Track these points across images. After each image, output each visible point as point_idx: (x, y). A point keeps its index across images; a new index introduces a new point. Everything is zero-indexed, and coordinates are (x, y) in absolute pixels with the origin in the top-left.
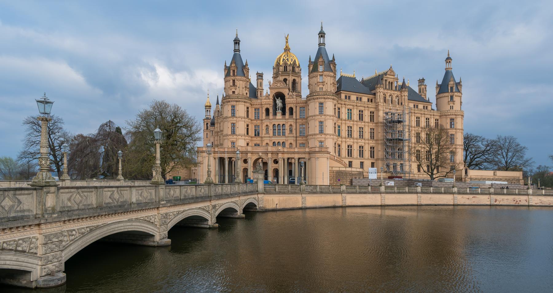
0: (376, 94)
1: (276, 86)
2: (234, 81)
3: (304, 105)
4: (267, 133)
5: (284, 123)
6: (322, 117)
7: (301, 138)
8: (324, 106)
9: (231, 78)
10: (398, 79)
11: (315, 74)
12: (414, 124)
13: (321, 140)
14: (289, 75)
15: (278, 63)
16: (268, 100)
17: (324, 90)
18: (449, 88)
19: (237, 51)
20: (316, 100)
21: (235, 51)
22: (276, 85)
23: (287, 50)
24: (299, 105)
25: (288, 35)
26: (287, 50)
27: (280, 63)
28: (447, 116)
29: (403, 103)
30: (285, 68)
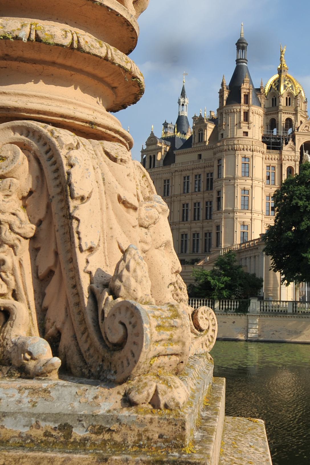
1: (307, 132)
2: (246, 114)
16: (293, 154)
19: (243, 62)
22: (307, 128)
26: (284, 71)
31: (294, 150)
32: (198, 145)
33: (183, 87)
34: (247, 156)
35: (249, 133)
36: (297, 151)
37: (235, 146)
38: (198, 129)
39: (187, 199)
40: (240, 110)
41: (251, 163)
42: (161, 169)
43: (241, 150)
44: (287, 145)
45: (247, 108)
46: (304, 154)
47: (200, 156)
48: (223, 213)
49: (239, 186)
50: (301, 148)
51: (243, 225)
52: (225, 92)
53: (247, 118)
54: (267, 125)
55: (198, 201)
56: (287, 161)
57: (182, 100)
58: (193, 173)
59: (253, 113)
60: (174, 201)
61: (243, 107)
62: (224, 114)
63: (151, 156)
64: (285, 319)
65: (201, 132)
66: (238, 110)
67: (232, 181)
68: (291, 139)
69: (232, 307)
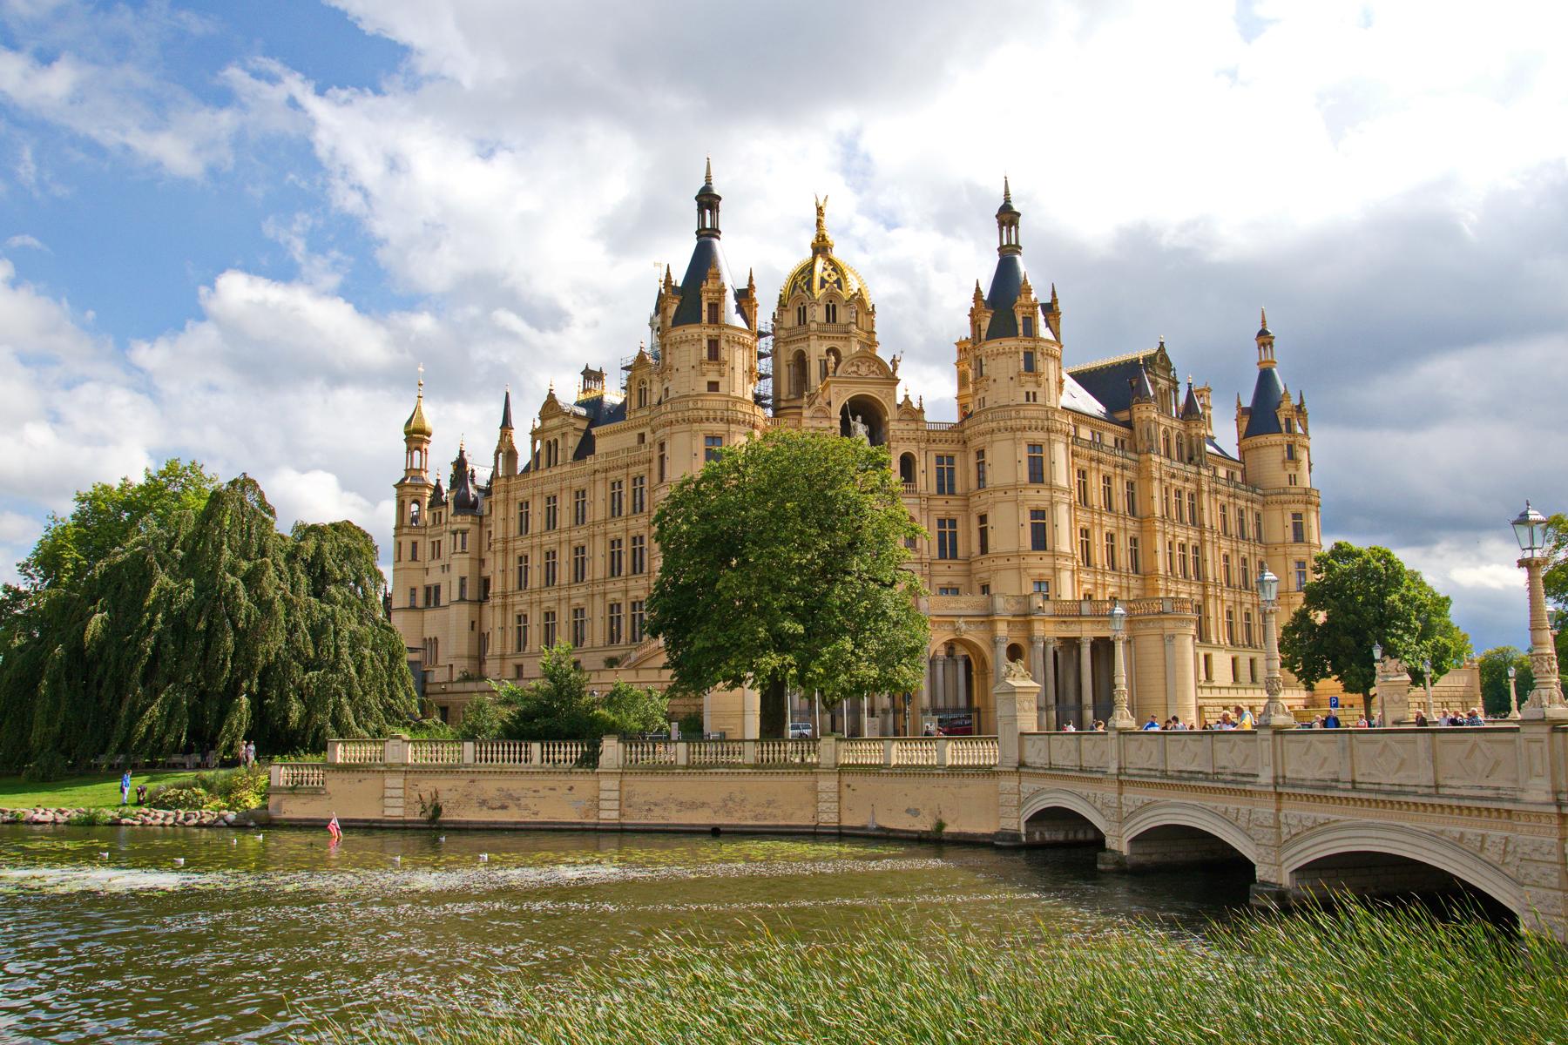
0: (1137, 429)
6: (1042, 493)
7: (945, 567)
8: (1045, 455)
9: (703, 331)
10: (1177, 383)
11: (1009, 343)
12: (1218, 526)
13: (1040, 575)
14: (847, 339)
15: (803, 291)
16: (826, 424)
17: (1040, 400)
18: (1282, 421)
20: (1019, 434)
21: (702, 233)
22: (854, 369)
23: (821, 247)
24: (934, 446)
25: (825, 200)
27: (813, 294)
28: (1285, 506)
29: (1197, 459)
30: (831, 312)
32: (638, 414)
35: (720, 384)
36: (835, 419)
38: (637, 380)
39: (616, 529)
42: (567, 469)
44: (812, 408)
46: (853, 423)
47: (642, 437)
50: (844, 412)
54: (789, 366)
55: (619, 537)
58: (628, 475)
59: (728, 341)
60: (594, 536)
62: (668, 346)
64: (670, 778)
65: (643, 386)
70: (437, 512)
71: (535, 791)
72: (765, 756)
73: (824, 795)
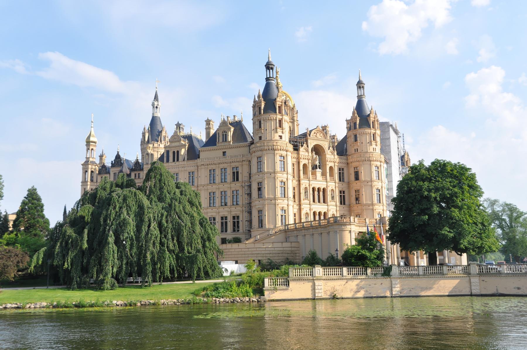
1: (315, 137)
2: (280, 121)
3: (344, 165)
4: (306, 197)
5: (325, 186)
16: (307, 154)
19: (271, 80)
22: (315, 134)
31: (307, 151)
32: (223, 144)
33: (156, 92)
34: (283, 155)
37: (275, 147)
39: (213, 188)
40: (276, 118)
41: (285, 160)
42: (185, 162)
43: (279, 150)
45: (281, 117)
47: (224, 153)
48: (266, 200)
49: (279, 179)
51: (282, 209)
52: (262, 103)
53: (280, 126)
56: (303, 160)
57: (156, 103)
61: (278, 116)
63: (174, 152)
65: (224, 133)
66: (275, 118)
67: (273, 175)
68: (305, 143)
69: (379, 272)
70: (104, 176)
71: (369, 285)
72: (426, 271)
73: (474, 284)
